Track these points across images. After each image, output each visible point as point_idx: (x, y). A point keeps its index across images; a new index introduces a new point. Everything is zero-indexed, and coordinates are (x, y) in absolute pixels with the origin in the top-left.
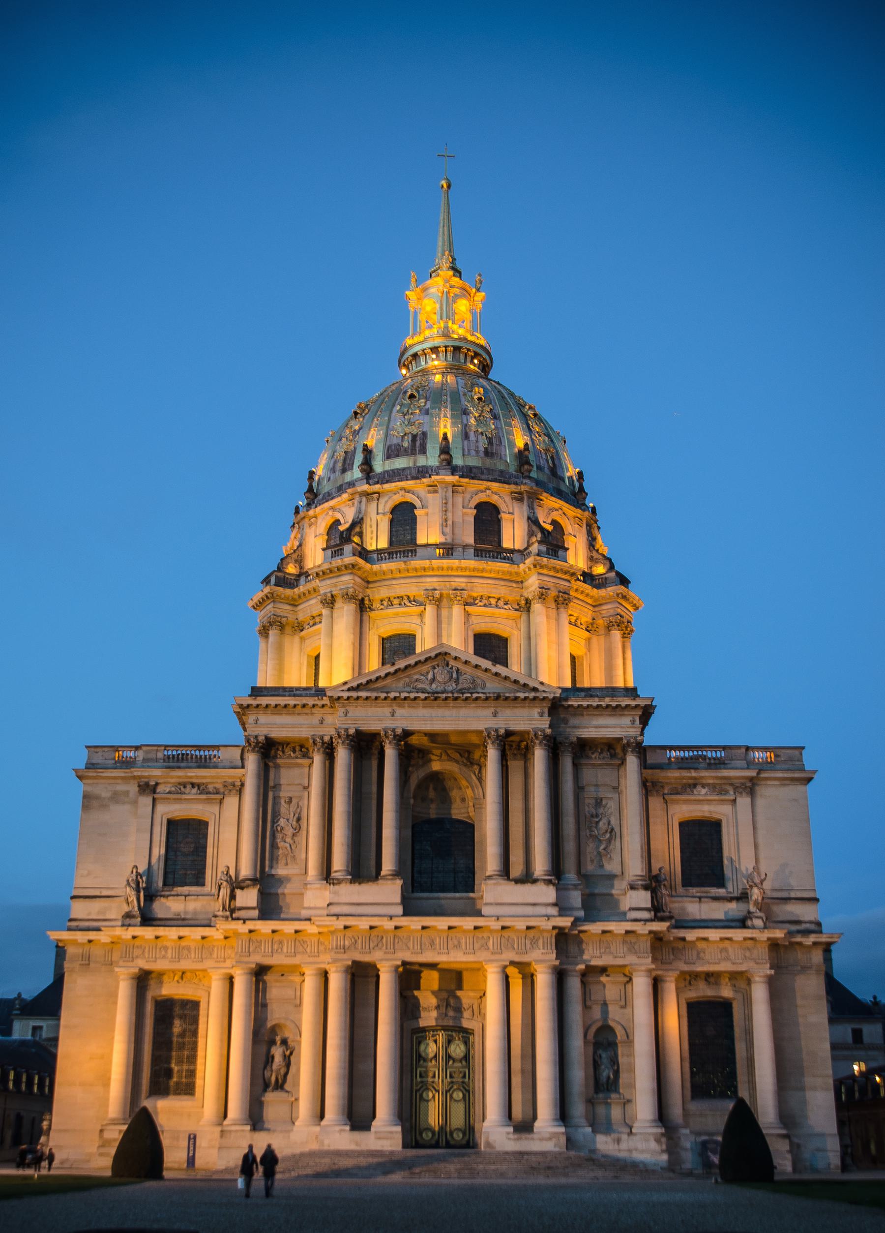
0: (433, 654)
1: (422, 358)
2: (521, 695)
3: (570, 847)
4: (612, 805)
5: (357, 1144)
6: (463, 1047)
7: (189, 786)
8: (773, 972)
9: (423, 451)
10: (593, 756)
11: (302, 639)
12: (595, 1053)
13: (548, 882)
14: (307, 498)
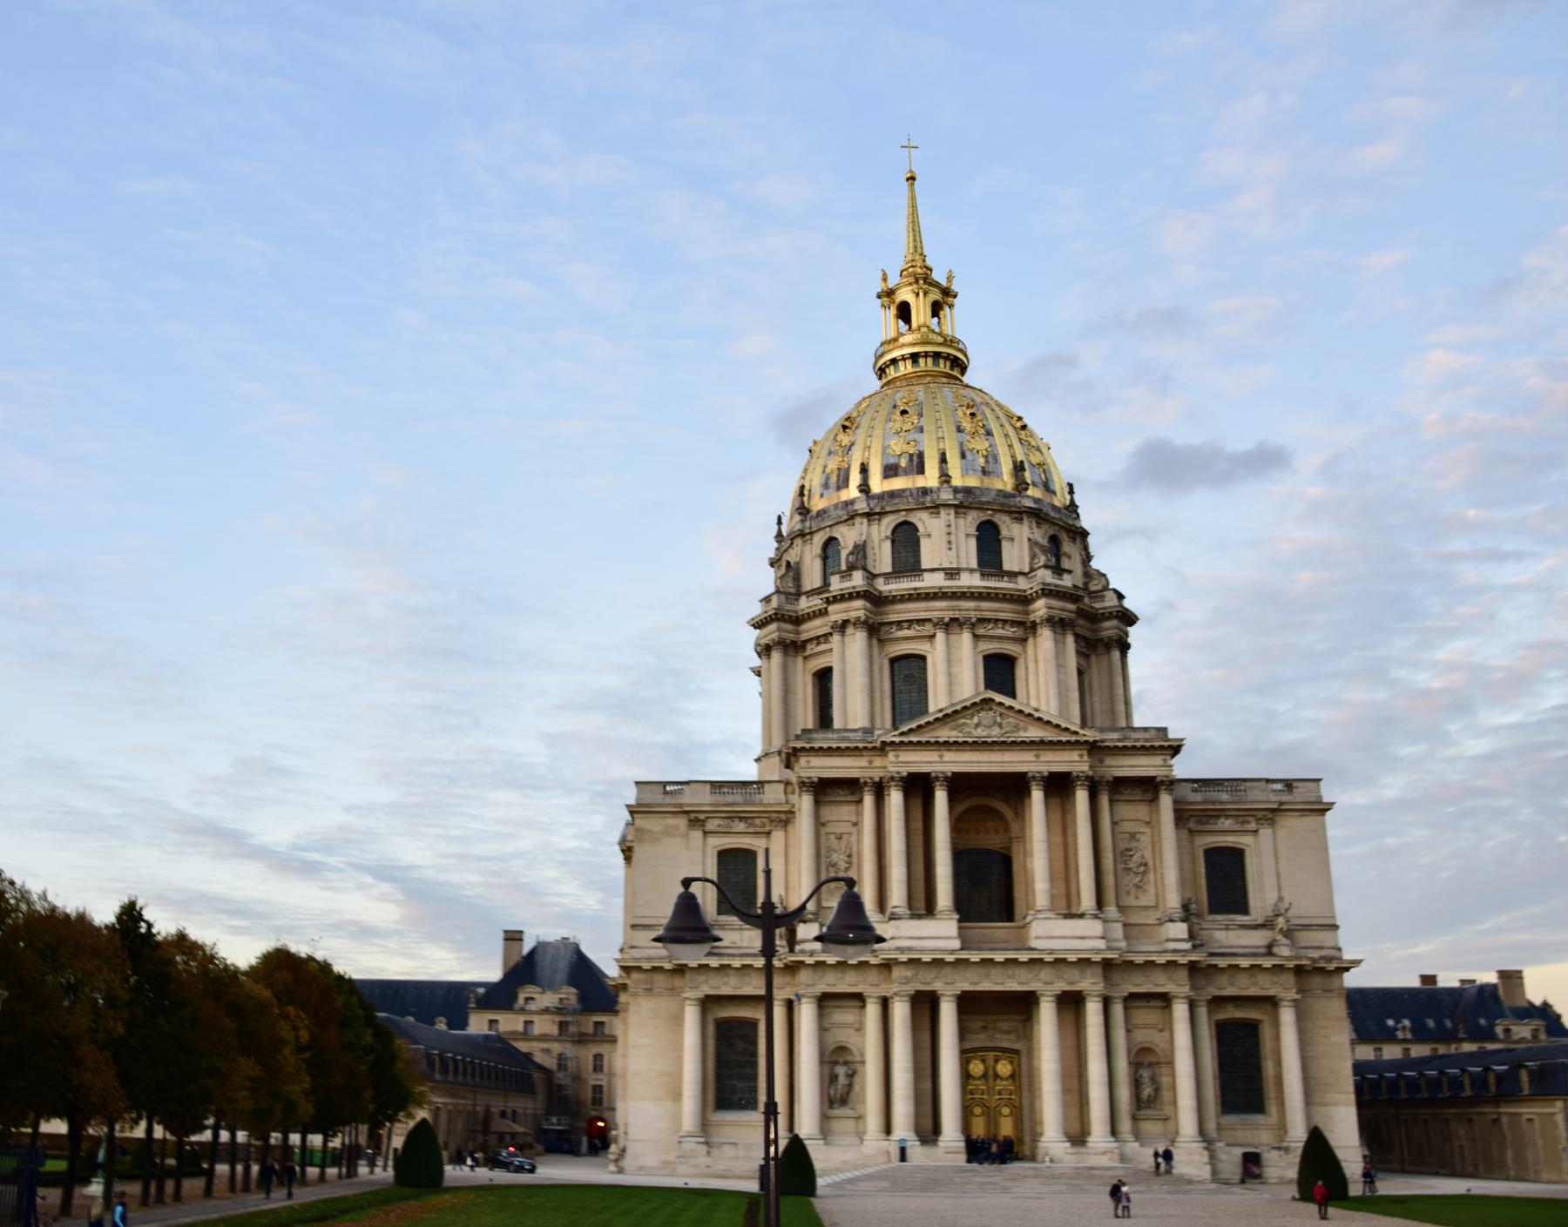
1: (901, 364)
2: (1064, 739)
3: (1109, 881)
4: (1145, 840)
6: (1009, 1067)
8: (1298, 996)
9: (921, 470)
11: (805, 658)
12: (1136, 1072)
13: (1096, 917)
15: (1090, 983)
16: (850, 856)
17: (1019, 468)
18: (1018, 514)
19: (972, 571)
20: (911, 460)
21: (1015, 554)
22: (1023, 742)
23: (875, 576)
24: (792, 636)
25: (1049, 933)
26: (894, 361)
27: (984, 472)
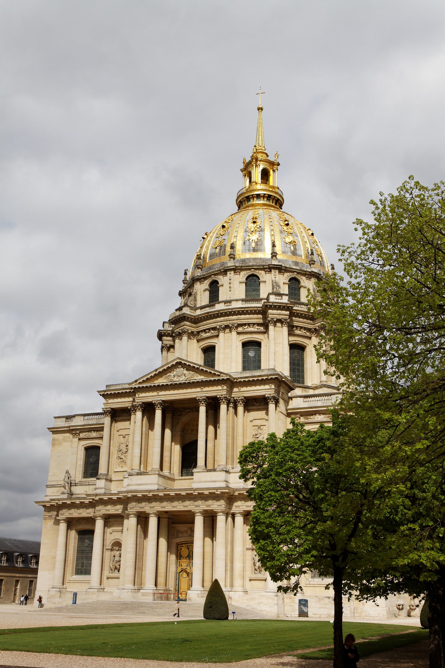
0: (174, 363)
1: (244, 203)
2: (212, 379)
5: (134, 598)
7: (93, 432)
10: (256, 405)
14: (184, 283)
15: (217, 506)
16: (127, 446)
17: (274, 246)
18: (269, 268)
19: (237, 300)
20: (220, 250)
21: (265, 290)
22: (193, 382)
23: (197, 309)
24: (172, 343)
25: (201, 480)
26: (240, 201)
27: (255, 250)
